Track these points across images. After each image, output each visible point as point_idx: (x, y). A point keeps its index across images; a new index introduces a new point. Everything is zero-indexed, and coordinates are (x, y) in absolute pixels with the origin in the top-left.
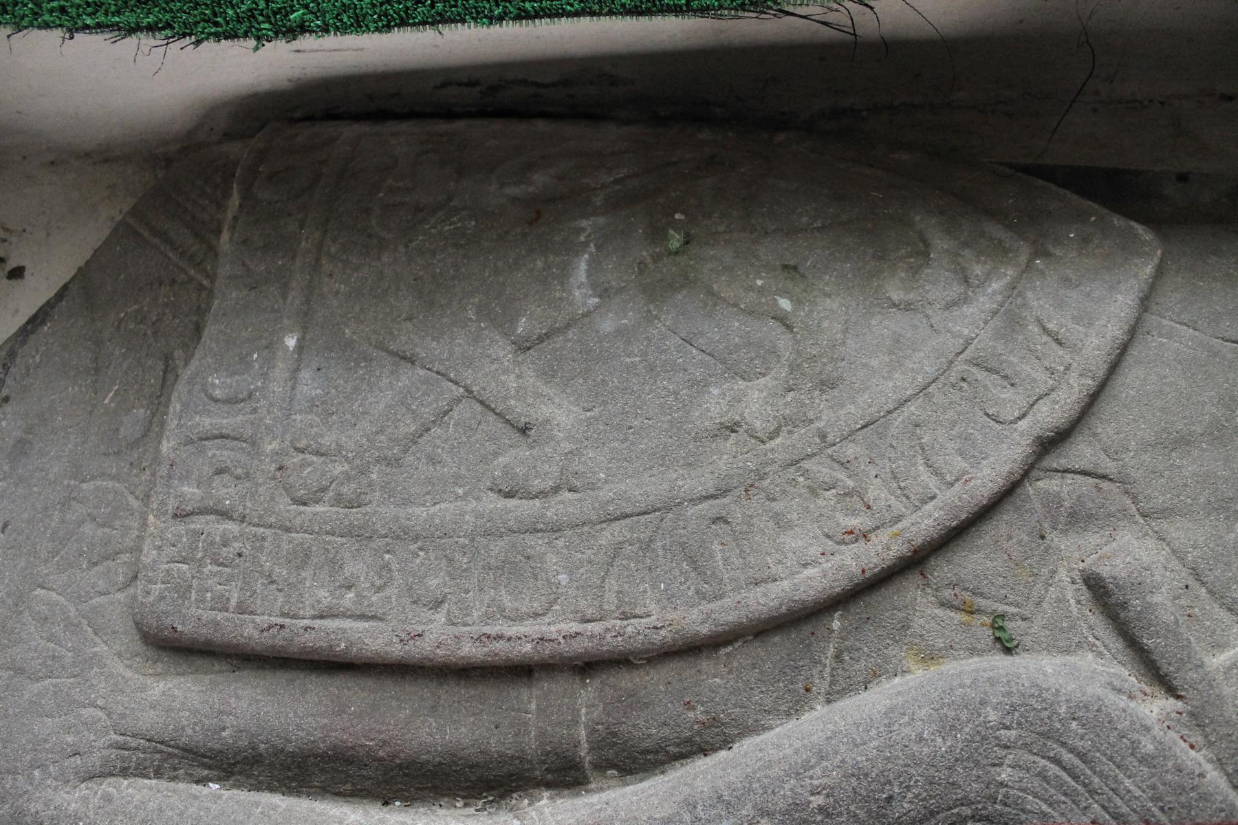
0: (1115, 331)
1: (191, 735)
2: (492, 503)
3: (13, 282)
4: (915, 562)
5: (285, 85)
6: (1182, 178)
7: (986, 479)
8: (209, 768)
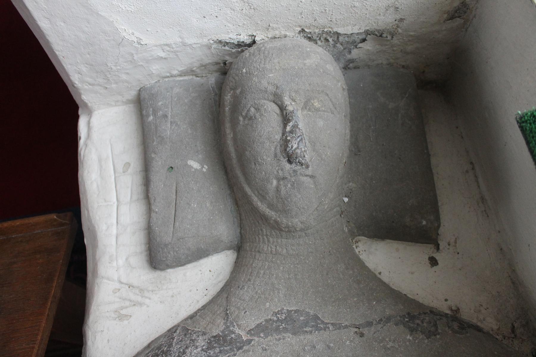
3: (428, 262)
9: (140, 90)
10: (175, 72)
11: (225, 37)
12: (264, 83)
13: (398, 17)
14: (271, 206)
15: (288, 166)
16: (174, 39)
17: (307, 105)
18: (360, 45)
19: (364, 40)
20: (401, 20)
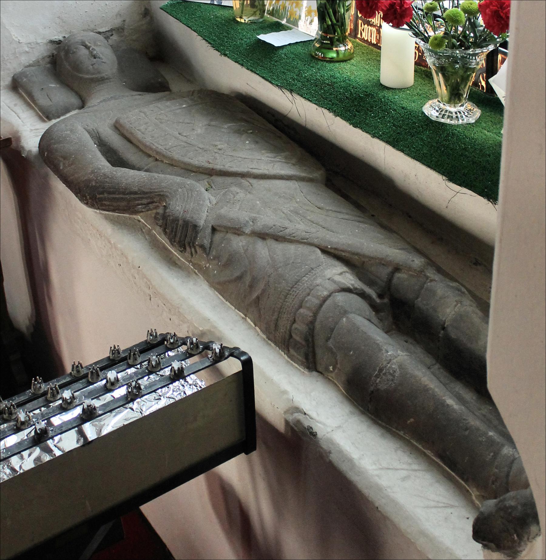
1: (103, 136)
2: (176, 133)
4: (211, 173)
5: (244, 93)
7: (235, 169)
8: (98, 142)
9: (13, 77)
10: (31, 62)
12: (76, 40)
13: (122, 19)
14: (93, 74)
15: (94, 60)
16: (32, 38)
18: (111, 37)
19: (112, 35)
20: (124, 21)
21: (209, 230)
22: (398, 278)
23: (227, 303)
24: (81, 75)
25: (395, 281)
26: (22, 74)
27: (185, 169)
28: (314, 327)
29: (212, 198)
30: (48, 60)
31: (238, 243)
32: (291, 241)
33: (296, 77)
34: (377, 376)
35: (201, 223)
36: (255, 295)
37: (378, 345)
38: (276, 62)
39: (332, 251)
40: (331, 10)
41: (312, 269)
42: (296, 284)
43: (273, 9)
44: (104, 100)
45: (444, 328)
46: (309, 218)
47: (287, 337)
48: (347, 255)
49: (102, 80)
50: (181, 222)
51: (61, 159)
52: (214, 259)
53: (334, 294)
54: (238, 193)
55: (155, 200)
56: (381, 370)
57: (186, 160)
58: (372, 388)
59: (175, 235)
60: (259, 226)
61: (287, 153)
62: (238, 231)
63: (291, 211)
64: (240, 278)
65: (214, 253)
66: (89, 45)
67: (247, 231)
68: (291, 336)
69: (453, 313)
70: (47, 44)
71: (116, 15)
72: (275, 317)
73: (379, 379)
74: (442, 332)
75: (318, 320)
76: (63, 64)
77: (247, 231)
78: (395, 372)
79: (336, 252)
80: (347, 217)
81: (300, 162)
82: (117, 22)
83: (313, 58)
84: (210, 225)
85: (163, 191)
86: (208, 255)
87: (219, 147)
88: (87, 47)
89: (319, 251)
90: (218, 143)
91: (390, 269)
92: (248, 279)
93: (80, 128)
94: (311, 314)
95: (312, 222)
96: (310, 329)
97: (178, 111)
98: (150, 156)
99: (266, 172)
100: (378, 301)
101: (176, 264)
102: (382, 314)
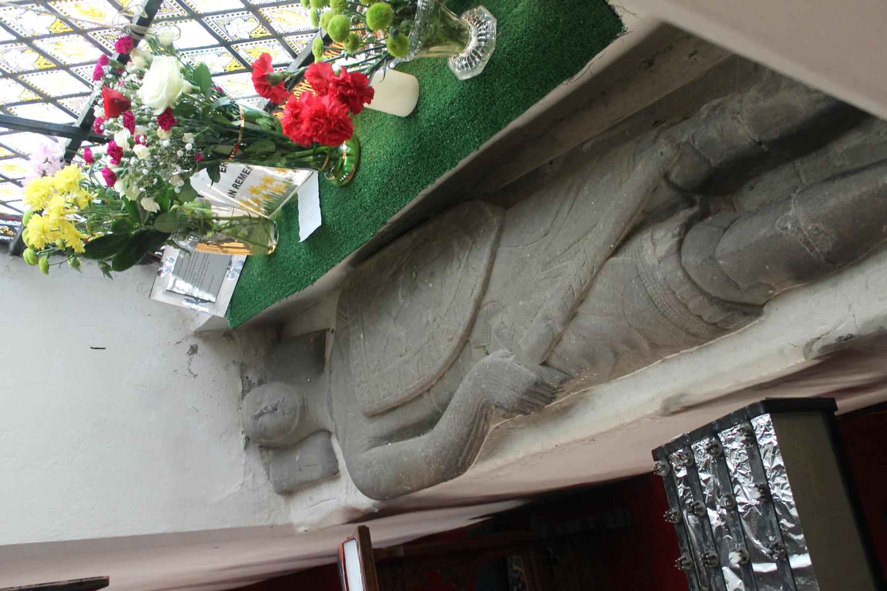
0: (485, 261)
2: (399, 359)
4: (465, 341)
6: (551, 163)
7: (468, 314)
11: (242, 445)
14: (295, 417)
17: (260, 404)
20: (234, 362)
21: (544, 369)
22: (677, 177)
23: (636, 372)
24: (293, 428)
25: (679, 182)
26: (276, 484)
27: (451, 366)
28: (716, 298)
29: (501, 351)
30: (264, 453)
31: (571, 343)
32: (590, 287)
33: (368, 213)
34: (812, 249)
35: (533, 376)
36: (645, 346)
37: (772, 236)
38: (340, 229)
39: (617, 243)
40: (297, 153)
41: (639, 276)
42: (654, 302)
43: (265, 208)
44: (331, 414)
45: (760, 143)
46: (558, 253)
47: (714, 328)
48: (628, 228)
49: (304, 408)
50: (525, 397)
51: (399, 487)
52: (580, 373)
53: (683, 264)
54: (502, 322)
55: (484, 413)
56: (807, 243)
57: (440, 363)
58: (822, 258)
59: (538, 405)
60: (558, 316)
61: (455, 243)
62: (557, 340)
63: (543, 270)
64: (616, 354)
65: (573, 371)
66: (259, 411)
67: (559, 329)
68: (715, 324)
69: (746, 127)
70: (248, 453)
71: (226, 370)
72: (684, 335)
73: (817, 249)
74: (763, 146)
75: (710, 292)
76: (277, 444)
77: (559, 329)
78: (817, 229)
79: (621, 239)
80: (567, 207)
81: (468, 231)
82: (234, 370)
83: (346, 186)
84: (539, 367)
85: (478, 404)
86: (572, 377)
87: (431, 320)
88: (262, 414)
89: (614, 259)
90: (424, 319)
91: (663, 183)
92: (622, 348)
93: (365, 455)
94: (701, 298)
95: (566, 251)
96: (717, 304)
97: (368, 346)
98: (421, 396)
99: (480, 280)
100: (696, 209)
101: (566, 408)
102: (712, 207)
